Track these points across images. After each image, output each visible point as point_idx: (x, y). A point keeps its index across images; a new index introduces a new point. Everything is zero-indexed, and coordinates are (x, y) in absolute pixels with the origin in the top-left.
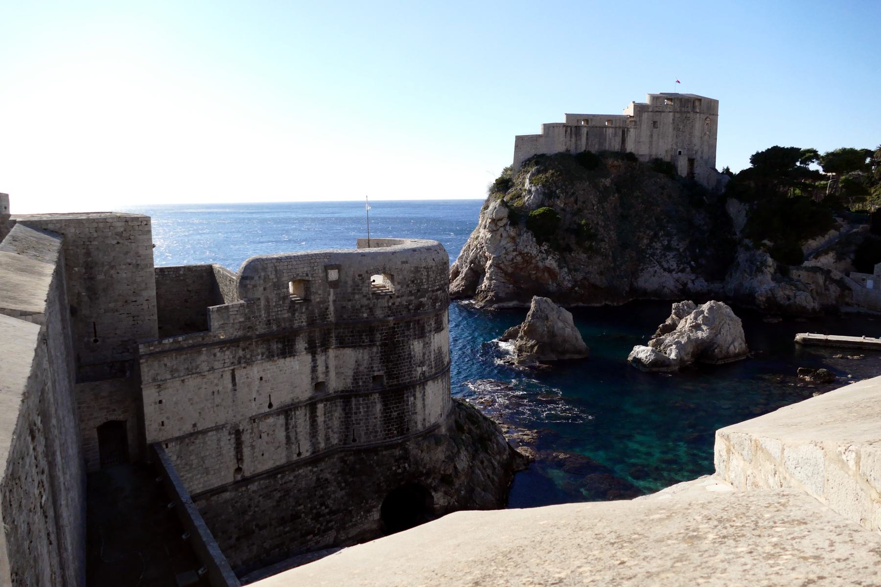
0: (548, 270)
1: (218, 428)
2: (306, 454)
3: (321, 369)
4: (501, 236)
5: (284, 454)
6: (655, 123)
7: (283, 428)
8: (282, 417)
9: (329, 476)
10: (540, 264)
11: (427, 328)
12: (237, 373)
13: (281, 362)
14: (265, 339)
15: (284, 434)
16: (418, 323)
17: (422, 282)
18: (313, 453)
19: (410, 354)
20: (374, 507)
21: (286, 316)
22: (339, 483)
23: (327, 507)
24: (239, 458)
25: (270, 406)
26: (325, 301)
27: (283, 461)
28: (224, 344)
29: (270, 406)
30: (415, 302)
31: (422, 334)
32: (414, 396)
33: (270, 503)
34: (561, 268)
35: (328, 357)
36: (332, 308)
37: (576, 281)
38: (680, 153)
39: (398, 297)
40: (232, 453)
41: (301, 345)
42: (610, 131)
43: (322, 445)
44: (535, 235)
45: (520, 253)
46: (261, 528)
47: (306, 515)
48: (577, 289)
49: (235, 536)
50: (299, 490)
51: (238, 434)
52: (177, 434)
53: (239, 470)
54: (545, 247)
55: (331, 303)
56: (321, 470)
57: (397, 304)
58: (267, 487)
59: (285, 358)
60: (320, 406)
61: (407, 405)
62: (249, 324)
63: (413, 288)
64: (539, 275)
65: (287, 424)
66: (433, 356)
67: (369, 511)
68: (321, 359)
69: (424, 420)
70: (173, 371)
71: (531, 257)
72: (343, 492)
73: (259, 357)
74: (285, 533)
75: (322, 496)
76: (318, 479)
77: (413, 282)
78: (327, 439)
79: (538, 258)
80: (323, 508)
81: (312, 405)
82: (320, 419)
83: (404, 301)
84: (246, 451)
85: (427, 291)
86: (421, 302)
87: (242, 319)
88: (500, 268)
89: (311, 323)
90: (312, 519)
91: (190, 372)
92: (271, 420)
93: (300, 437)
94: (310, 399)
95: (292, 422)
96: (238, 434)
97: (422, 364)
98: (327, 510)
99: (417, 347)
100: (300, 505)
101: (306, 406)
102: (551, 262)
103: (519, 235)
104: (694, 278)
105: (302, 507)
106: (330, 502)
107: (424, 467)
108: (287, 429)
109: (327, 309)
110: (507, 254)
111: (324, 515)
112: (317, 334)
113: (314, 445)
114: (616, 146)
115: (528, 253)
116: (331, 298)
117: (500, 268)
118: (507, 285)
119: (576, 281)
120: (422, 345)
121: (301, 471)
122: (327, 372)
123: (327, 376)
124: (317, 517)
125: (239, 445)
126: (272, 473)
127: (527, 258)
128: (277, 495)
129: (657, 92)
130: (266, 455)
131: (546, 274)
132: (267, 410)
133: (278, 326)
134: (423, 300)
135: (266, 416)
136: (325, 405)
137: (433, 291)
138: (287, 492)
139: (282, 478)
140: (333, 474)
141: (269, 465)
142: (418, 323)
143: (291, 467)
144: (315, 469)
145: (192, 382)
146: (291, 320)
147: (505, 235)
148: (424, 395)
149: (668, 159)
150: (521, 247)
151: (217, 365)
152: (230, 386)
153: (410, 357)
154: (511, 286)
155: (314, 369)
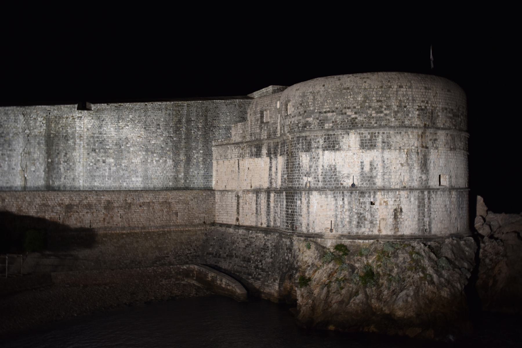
1: (232, 191)
2: (264, 226)
3: (274, 169)
5: (255, 220)
7: (255, 203)
8: (255, 195)
9: (270, 245)
11: (314, 145)
12: (241, 162)
13: (256, 159)
14: (250, 144)
15: (255, 206)
16: (306, 139)
17: (308, 105)
18: (268, 226)
19: (299, 164)
20: (277, 279)
21: (258, 131)
22: (272, 253)
23: (262, 264)
24: (238, 213)
25: (251, 187)
26: (275, 123)
27: (254, 224)
28: (237, 144)
29: (251, 187)
30: (303, 121)
31: (308, 149)
32: (301, 199)
33: (242, 245)
35: (277, 163)
36: (279, 128)
39: (293, 117)
40: (236, 208)
41: (264, 151)
43: (272, 224)
46: (237, 257)
47: (253, 263)
49: (227, 253)
50: (255, 246)
51: (238, 197)
52: (221, 189)
53: (238, 220)
55: (279, 124)
56: (268, 240)
57: (292, 123)
58: (244, 235)
59: (257, 157)
60: (272, 195)
61: (296, 206)
62: (244, 134)
63: (301, 110)
65: (257, 201)
66: (320, 171)
67: (274, 281)
68: (274, 162)
69: (308, 225)
70: (221, 156)
72: (271, 260)
73: (247, 155)
74: (244, 267)
75: (262, 256)
76: (265, 244)
77: (301, 104)
78: (275, 221)
80: (260, 263)
81: (268, 191)
82: (272, 205)
83: (295, 120)
84: (241, 209)
85: (313, 112)
86: (307, 121)
87: (241, 132)
89: (269, 137)
90: (255, 267)
91: (226, 157)
92: (250, 195)
93: (262, 212)
94: (268, 188)
95: (259, 200)
96: (238, 197)
97: (308, 174)
98: (261, 266)
99: (304, 159)
100: (253, 255)
101: (265, 191)
105: (253, 256)
106: (264, 262)
107: (297, 263)
108: (257, 204)
109: (277, 128)
111: (259, 268)
112: (272, 145)
113: (268, 221)
116: (279, 121)
120: (309, 158)
121: (259, 234)
122: (276, 173)
123: (276, 175)
124: (257, 267)
125: (238, 204)
126: (248, 228)
128: (247, 243)
130: (248, 215)
132: (249, 188)
133: (255, 137)
134: (310, 120)
135: (248, 191)
136: (275, 195)
137: (320, 112)
138: (251, 243)
139: (252, 233)
140: (272, 246)
141: (247, 223)
142: (306, 139)
143: (256, 229)
144: (265, 237)
145: (227, 162)
146: (260, 134)
148: (308, 203)
151: (233, 156)
152: (237, 169)
153: (299, 166)
155: (271, 168)
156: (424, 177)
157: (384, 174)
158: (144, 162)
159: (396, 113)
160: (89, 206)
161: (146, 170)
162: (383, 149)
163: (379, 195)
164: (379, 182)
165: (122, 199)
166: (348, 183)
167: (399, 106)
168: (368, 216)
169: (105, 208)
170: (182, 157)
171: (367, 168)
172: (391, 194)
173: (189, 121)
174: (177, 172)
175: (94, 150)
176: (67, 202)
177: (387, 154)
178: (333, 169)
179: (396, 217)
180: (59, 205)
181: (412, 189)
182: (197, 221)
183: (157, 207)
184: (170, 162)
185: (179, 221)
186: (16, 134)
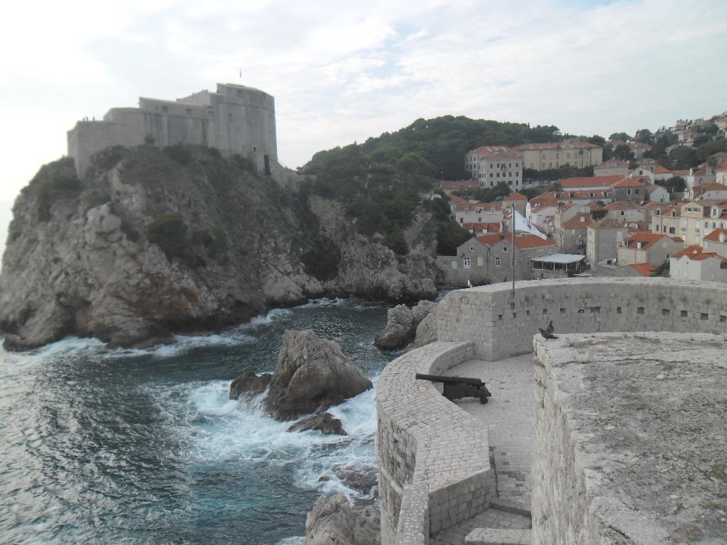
0: (184, 291)
4: (115, 254)
6: (230, 115)
10: (176, 286)
34: (199, 287)
37: (220, 301)
38: (255, 148)
42: (190, 122)
44: (163, 248)
45: (148, 275)
48: (223, 309)
54: (175, 266)
64: (175, 298)
71: (163, 278)
79: (172, 279)
88: (121, 298)
102: (188, 282)
103: (141, 251)
104: (308, 279)
110: (129, 277)
114: (199, 141)
115: (158, 273)
117: (121, 298)
118: (135, 319)
119: (220, 301)
127: (157, 280)
129: (225, 82)
131: (183, 297)
147: (120, 252)
149: (245, 155)
150: (147, 266)
154: (141, 319)
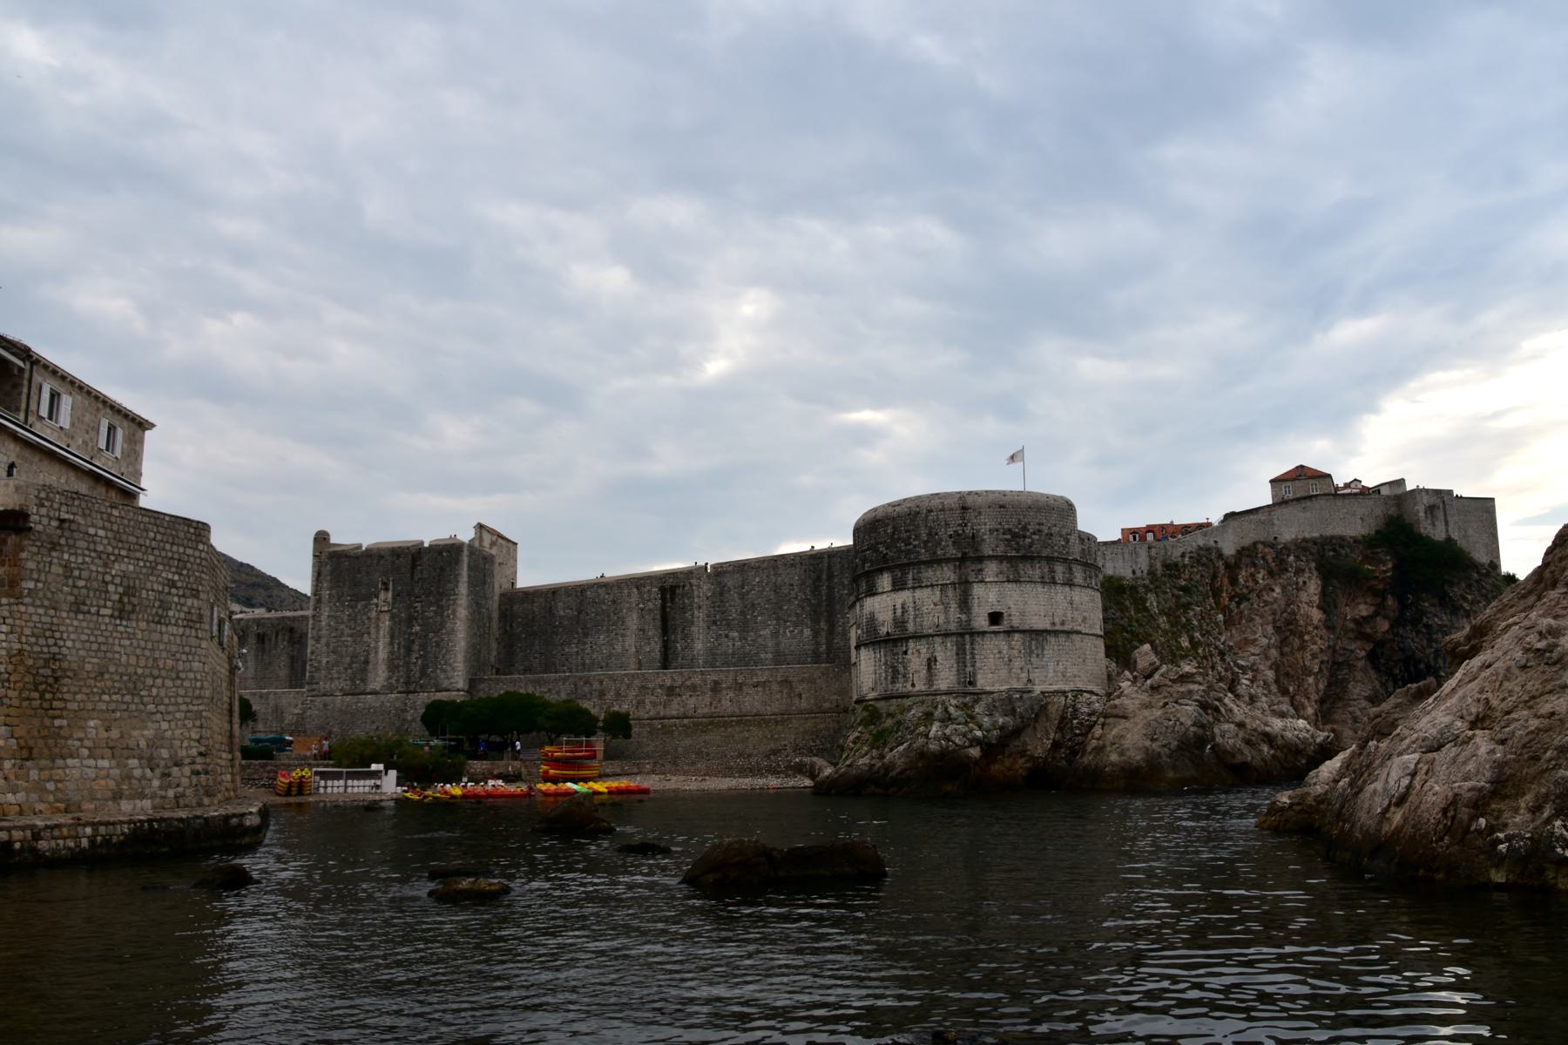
156: (964, 617)
157: (916, 617)
158: (775, 634)
159: (926, 542)
160: (694, 688)
161: (778, 644)
162: (914, 588)
163: (911, 644)
164: (911, 627)
165: (730, 679)
166: (883, 630)
167: (929, 534)
168: (901, 669)
169: (712, 690)
170: (823, 625)
171: (899, 612)
172: (924, 641)
173: (830, 577)
174: (818, 644)
175: (714, 623)
176: (668, 683)
177: (918, 593)
178: (872, 614)
179: (929, 668)
180: (661, 686)
181: (946, 635)
182: (827, 705)
183: (775, 687)
184: (807, 632)
185: (804, 705)
186: (630, 610)
